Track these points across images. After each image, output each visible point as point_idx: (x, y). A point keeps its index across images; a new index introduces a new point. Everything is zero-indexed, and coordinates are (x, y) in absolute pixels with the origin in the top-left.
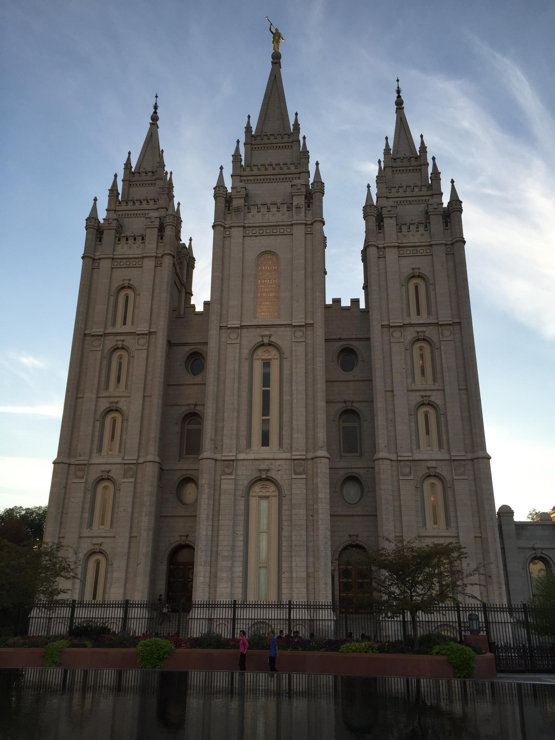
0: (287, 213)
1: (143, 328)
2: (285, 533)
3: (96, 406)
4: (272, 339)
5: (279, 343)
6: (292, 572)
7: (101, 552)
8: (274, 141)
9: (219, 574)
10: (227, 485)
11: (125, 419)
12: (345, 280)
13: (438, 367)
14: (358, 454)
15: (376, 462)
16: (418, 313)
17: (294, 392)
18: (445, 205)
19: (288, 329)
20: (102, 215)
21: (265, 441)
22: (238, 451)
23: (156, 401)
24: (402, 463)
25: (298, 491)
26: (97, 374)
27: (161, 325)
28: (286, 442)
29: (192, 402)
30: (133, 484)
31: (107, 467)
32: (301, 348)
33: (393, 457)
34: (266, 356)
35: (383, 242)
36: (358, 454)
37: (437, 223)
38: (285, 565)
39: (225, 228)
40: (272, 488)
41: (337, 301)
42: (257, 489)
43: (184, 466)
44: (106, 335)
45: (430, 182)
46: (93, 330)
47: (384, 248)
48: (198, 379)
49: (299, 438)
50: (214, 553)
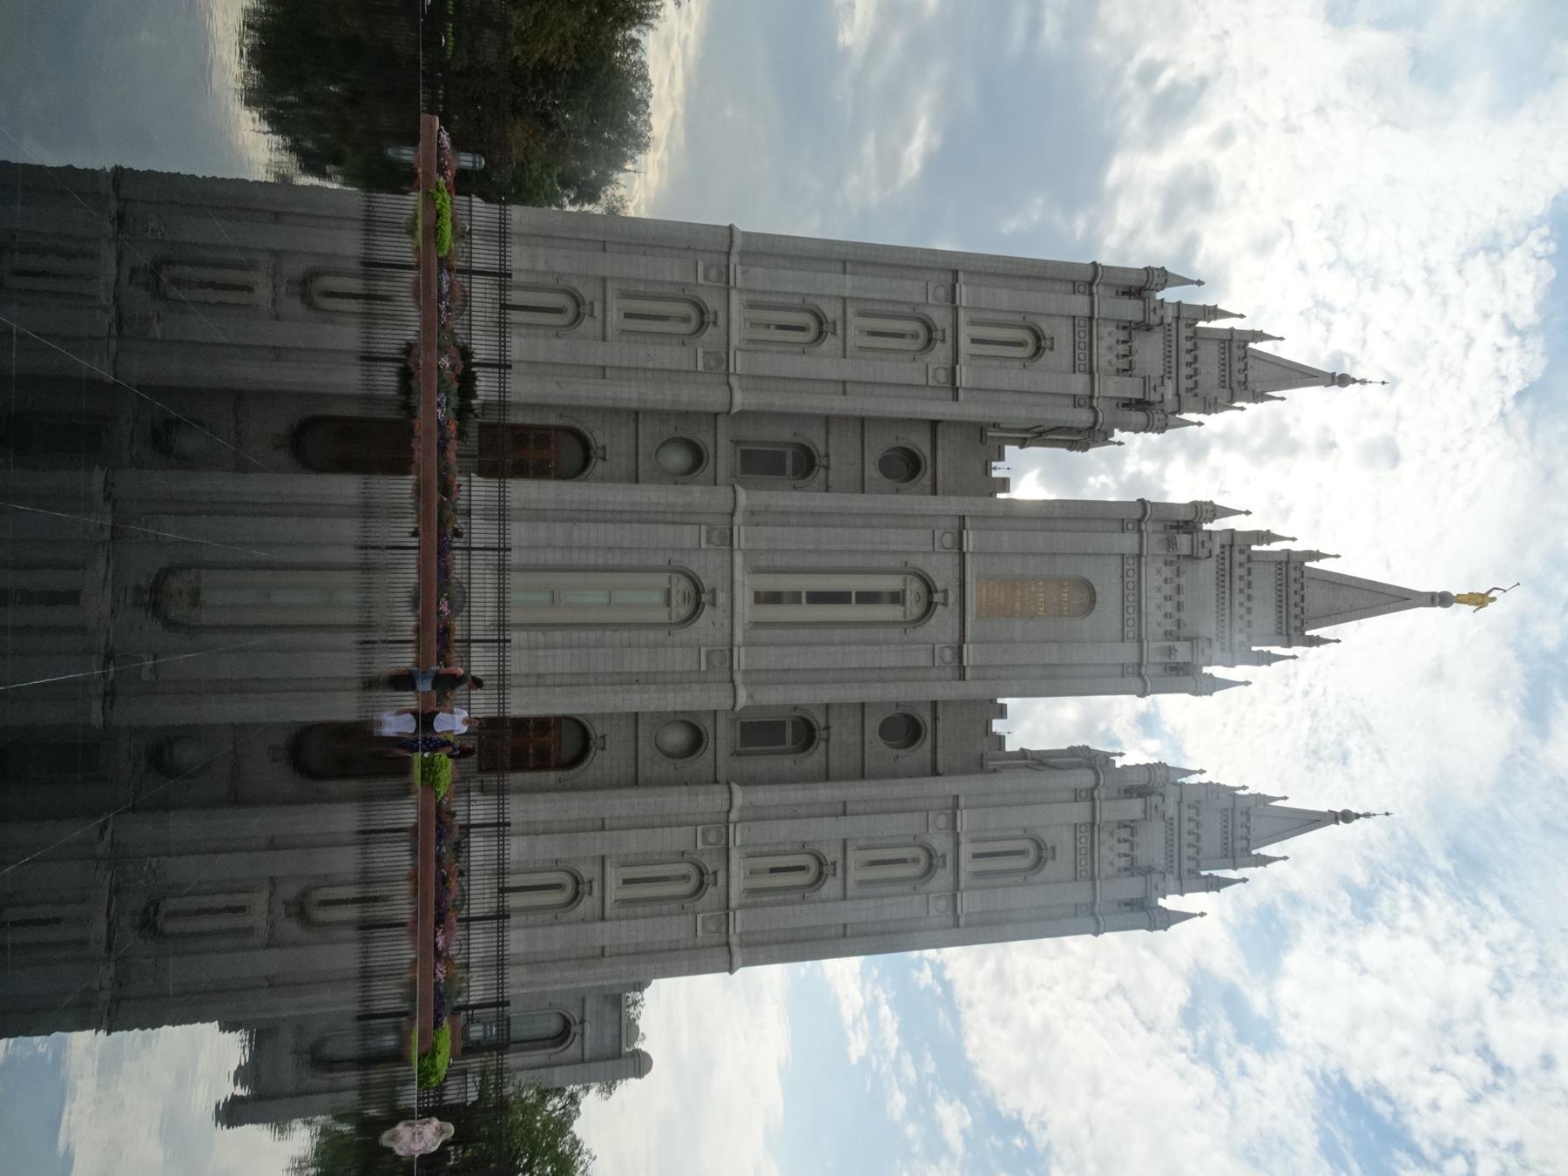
0: (1161, 631)
1: (965, 376)
2: (608, 634)
3: (830, 297)
4: (939, 608)
5: (933, 621)
6: (546, 648)
7: (578, 316)
8: (1292, 602)
9: (542, 525)
11: (804, 348)
13: (884, 890)
14: (739, 748)
15: (725, 787)
16: (976, 856)
17: (847, 649)
18: (1161, 902)
19: (957, 636)
20: (1169, 295)
22: (747, 553)
23: (836, 404)
24: (723, 830)
25: (678, 659)
26: (886, 297)
27: (969, 410)
28: (763, 634)
29: (833, 462)
30: (692, 368)
31: (721, 321)
32: (922, 659)
33: (734, 816)
34: (910, 597)
35: (1103, 796)
36: (739, 748)
38: (557, 636)
39: (1140, 521)
40: (683, 611)
41: (1002, 712)
42: (684, 585)
43: (725, 458)
44: (955, 310)
45: (1204, 873)
46: (964, 288)
47: (1093, 799)
48: (872, 471)
49: (769, 658)
50: (577, 515)
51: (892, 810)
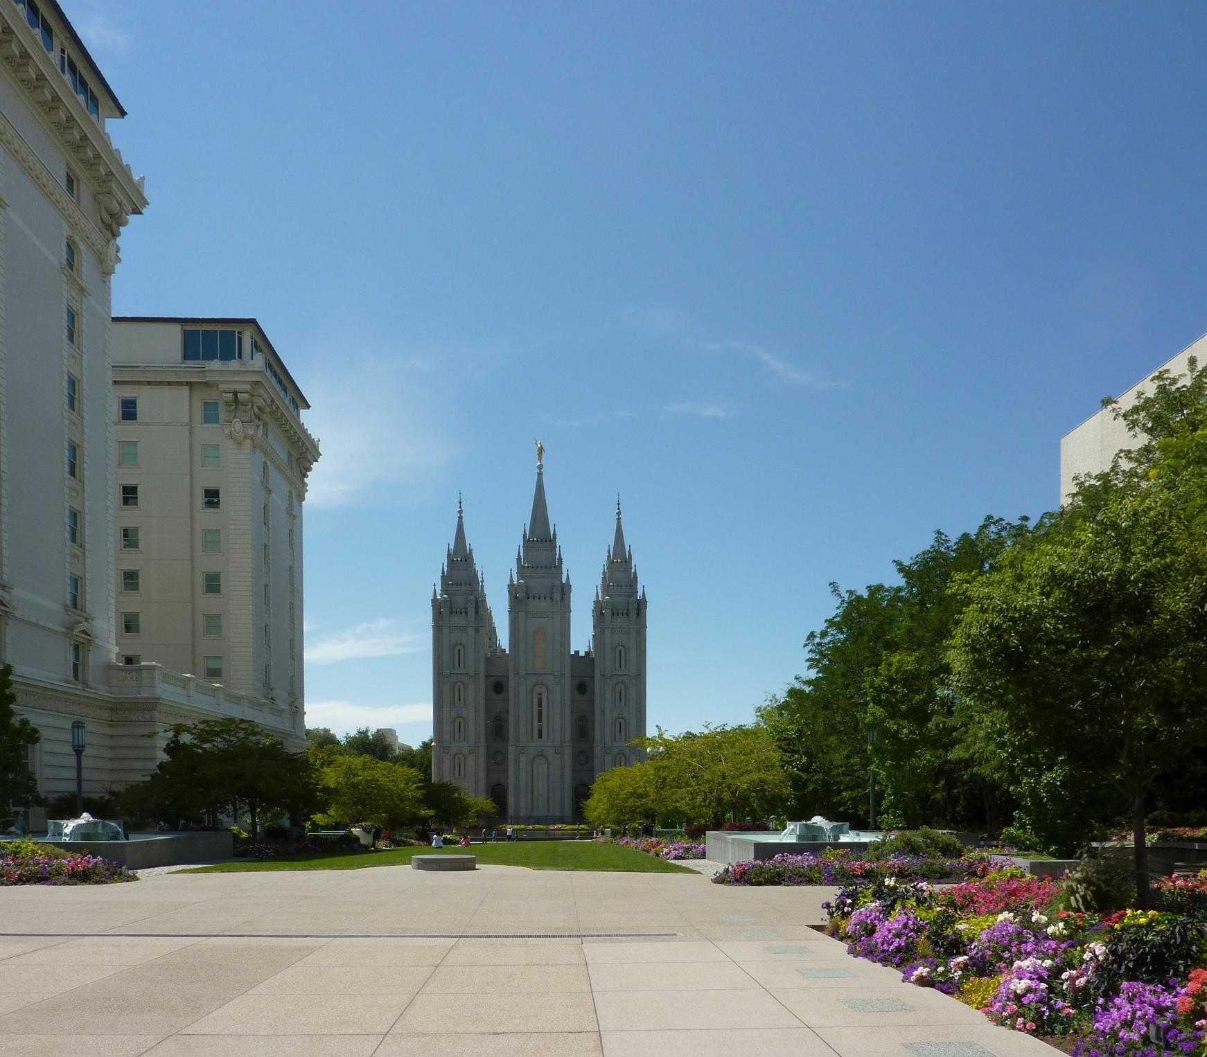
10: (523, 758)
12: (581, 639)
21: (540, 736)
23: (482, 713)
37: (633, 613)
41: (577, 652)
48: (501, 697)
51: (604, 695)
